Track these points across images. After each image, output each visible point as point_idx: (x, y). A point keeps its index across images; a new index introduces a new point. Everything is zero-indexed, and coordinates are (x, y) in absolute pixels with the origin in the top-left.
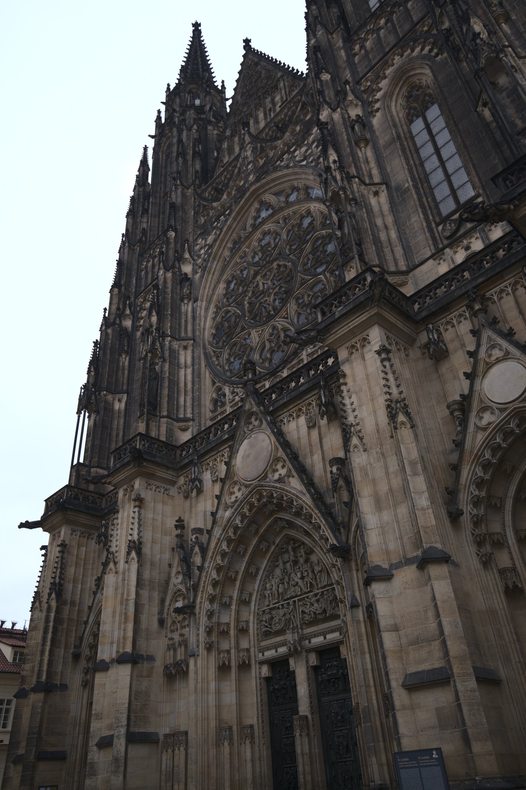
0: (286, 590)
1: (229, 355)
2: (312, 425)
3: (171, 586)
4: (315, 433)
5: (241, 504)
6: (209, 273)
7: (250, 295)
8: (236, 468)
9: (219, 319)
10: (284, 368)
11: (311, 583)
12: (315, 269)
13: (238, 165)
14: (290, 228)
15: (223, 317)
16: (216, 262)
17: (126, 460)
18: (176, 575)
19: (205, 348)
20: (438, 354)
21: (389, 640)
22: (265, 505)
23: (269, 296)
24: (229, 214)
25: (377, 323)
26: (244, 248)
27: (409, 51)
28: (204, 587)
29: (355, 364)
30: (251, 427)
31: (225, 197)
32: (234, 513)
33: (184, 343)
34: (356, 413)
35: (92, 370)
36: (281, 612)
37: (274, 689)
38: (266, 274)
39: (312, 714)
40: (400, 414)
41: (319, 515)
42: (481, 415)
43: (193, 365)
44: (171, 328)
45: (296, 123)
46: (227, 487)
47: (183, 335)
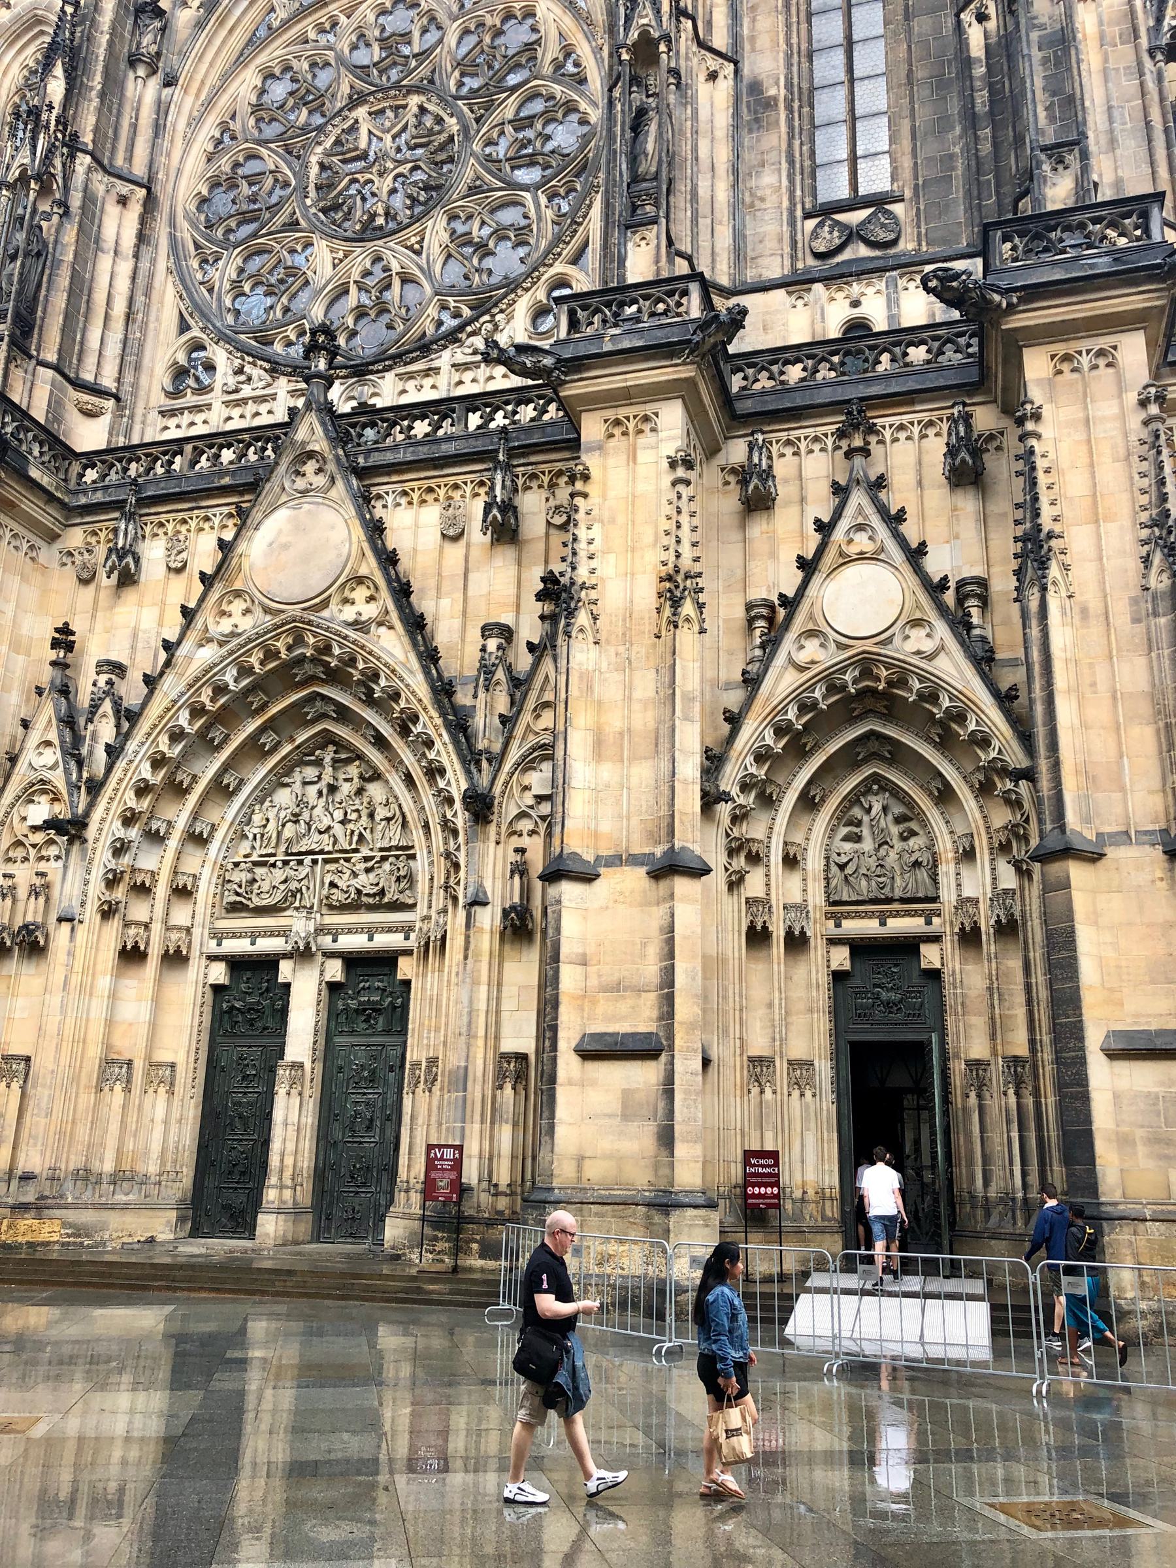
0: (299, 837)
1: (241, 271)
2: (453, 535)
3: (21, 767)
4: (455, 552)
5: (246, 644)
6: (221, 22)
7: (328, 143)
8: (246, 565)
9: (224, 164)
10: (388, 369)
11: (361, 835)
12: (513, 168)
15: (237, 165)
18: (38, 746)
19: (173, 223)
20: (757, 500)
21: (569, 978)
22: (301, 660)
25: (682, 397)
28: (116, 790)
29: (611, 462)
30: (301, 484)
32: (224, 658)
34: (593, 564)
36: (279, 874)
37: (233, 1008)
38: (382, 112)
39: (313, 1061)
40: (688, 600)
42: (803, 642)
43: (136, 256)
44: (96, 130)
46: (214, 595)
47: (119, 161)
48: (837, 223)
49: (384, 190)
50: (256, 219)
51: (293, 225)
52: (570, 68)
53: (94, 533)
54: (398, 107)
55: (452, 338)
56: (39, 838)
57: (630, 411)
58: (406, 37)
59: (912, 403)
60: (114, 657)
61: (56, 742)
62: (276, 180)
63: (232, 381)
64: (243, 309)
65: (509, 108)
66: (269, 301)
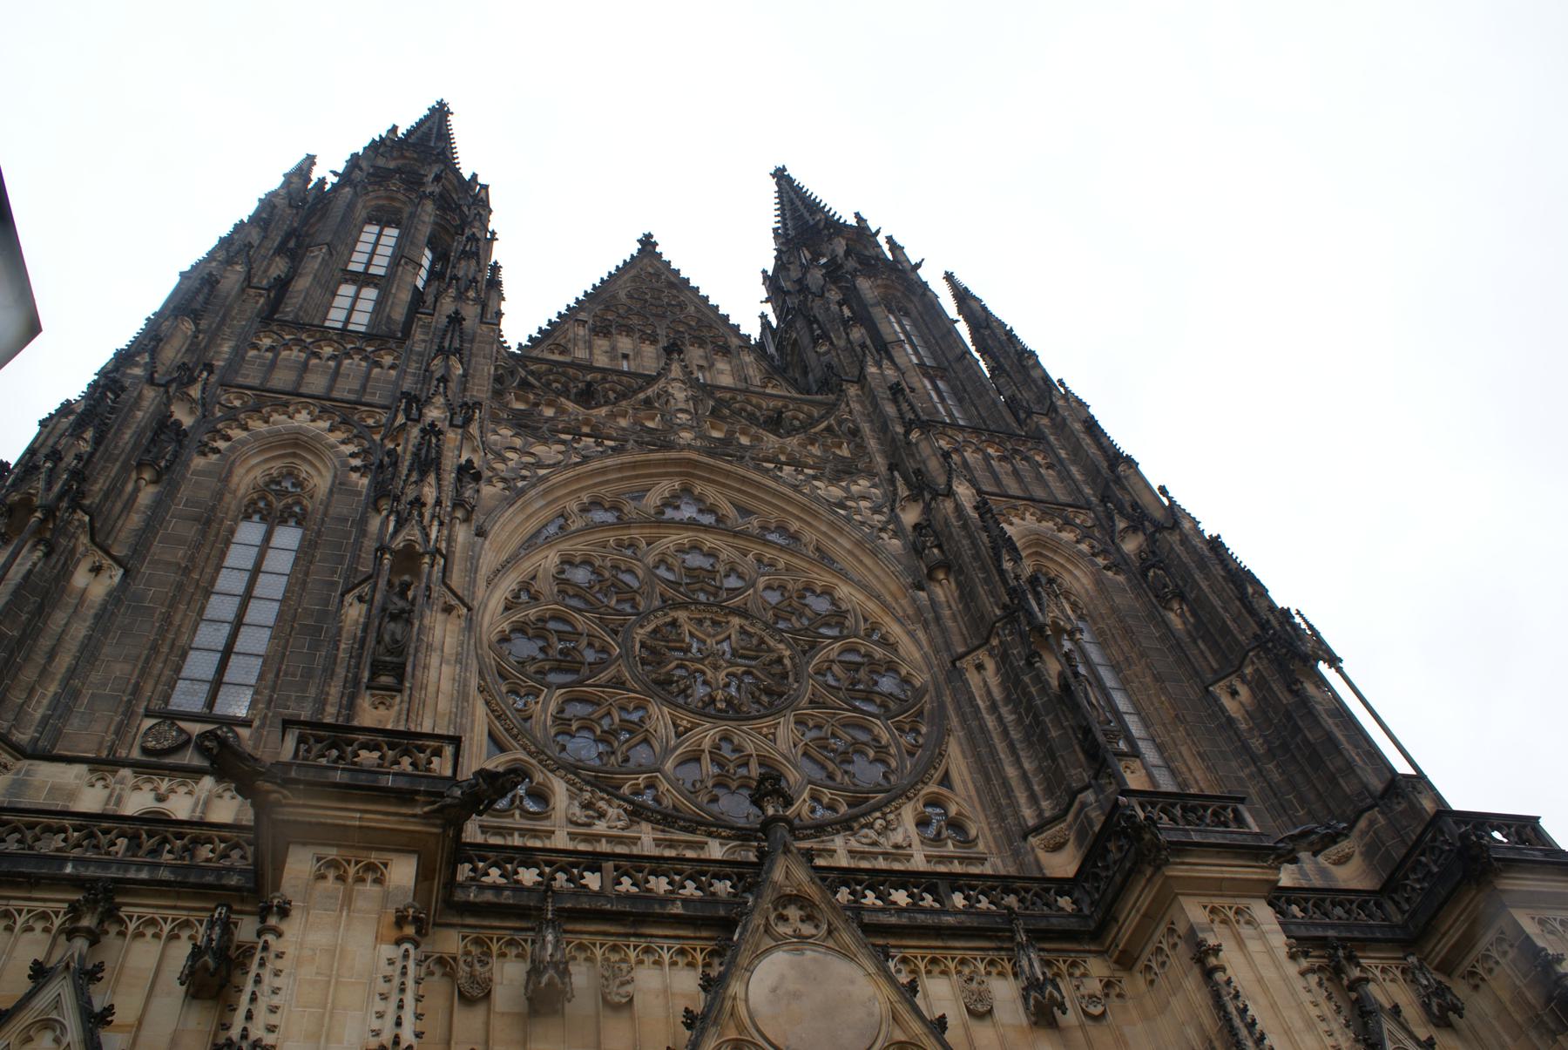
1: (562, 711)
2: (980, 1012)
6: (523, 508)
7: (650, 628)
9: (533, 613)
13: (650, 392)
14: (776, 585)
15: (541, 619)
16: (542, 502)
23: (716, 668)
24: (613, 449)
26: (635, 533)
27: (1051, 524)
30: (782, 929)
31: (603, 411)
33: (454, 602)
35: (89, 434)
38: (700, 622)
43: (458, 661)
49: (720, 681)
50: (577, 672)
52: (875, 637)
53: (478, 942)
55: (846, 825)
57: (1226, 902)
58: (712, 572)
62: (590, 645)
63: (579, 814)
64: (569, 746)
66: (601, 748)
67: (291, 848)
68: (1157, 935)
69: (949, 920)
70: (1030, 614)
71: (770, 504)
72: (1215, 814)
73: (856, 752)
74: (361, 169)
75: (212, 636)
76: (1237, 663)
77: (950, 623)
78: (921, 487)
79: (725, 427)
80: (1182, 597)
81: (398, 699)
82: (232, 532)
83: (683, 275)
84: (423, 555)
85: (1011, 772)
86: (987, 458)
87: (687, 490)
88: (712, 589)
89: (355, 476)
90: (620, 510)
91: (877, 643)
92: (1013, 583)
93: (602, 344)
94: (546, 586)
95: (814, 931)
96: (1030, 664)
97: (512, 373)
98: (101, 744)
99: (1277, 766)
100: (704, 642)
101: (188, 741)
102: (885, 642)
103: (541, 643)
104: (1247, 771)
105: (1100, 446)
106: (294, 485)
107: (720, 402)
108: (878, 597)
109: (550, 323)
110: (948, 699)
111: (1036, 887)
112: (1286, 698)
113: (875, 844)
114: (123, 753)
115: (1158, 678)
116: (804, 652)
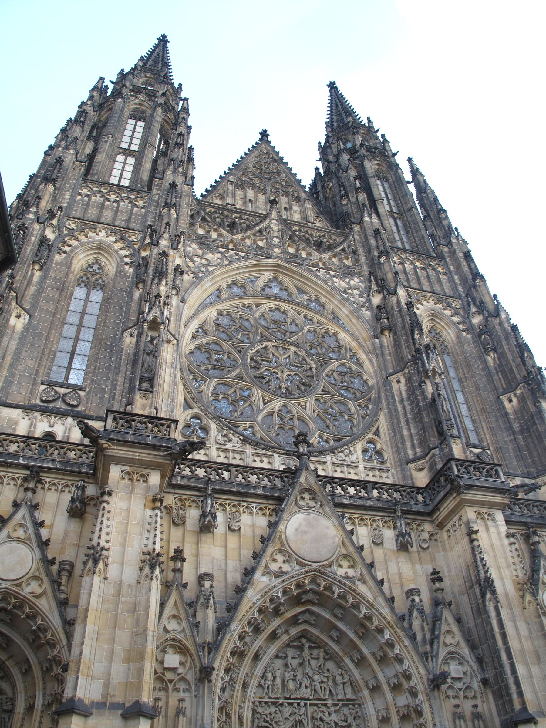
1: (215, 389)
2: (378, 542)
4: (378, 553)
7: (254, 350)
9: (205, 340)
11: (330, 690)
13: (261, 226)
15: (207, 343)
16: (210, 284)
17: (149, 441)
23: (282, 372)
24: (243, 257)
27: (441, 306)
30: (302, 503)
31: (240, 236)
32: (279, 584)
33: (171, 338)
41: (401, 634)
45: (335, 256)
46: (269, 551)
48: (471, 451)
51: (240, 377)
52: (354, 360)
53: (180, 500)
54: (283, 348)
55: (332, 451)
56: (169, 676)
57: (485, 510)
58: (284, 323)
59: (542, 528)
60: (202, 570)
61: (183, 616)
62: (228, 357)
65: (334, 365)
66: (231, 407)
67: (112, 466)
68: (455, 519)
69: (370, 503)
70: (423, 363)
71: (312, 288)
72: (487, 471)
73: (340, 415)
74: (126, 87)
75: (66, 345)
76: (514, 387)
77: (388, 357)
78: (382, 286)
79: (295, 247)
80: (495, 351)
81: (151, 396)
82: (72, 293)
83: (281, 155)
84: (161, 324)
85: (405, 432)
86: (415, 268)
87: (275, 278)
88: (284, 332)
89: (127, 267)
90: (244, 287)
91: (354, 363)
92: (417, 346)
93: (239, 193)
94: (211, 328)
95: (314, 505)
96: (420, 386)
97: (198, 213)
98: (25, 398)
99: (523, 438)
100: (278, 358)
101: (59, 397)
102: (358, 363)
103: (207, 355)
104: (510, 438)
105: (470, 267)
106: (99, 268)
107: (294, 232)
108: (357, 340)
109: (216, 182)
110: (382, 394)
111: (409, 490)
112: (532, 409)
113: (343, 460)
114: (33, 402)
115: (478, 389)
116: (322, 366)
